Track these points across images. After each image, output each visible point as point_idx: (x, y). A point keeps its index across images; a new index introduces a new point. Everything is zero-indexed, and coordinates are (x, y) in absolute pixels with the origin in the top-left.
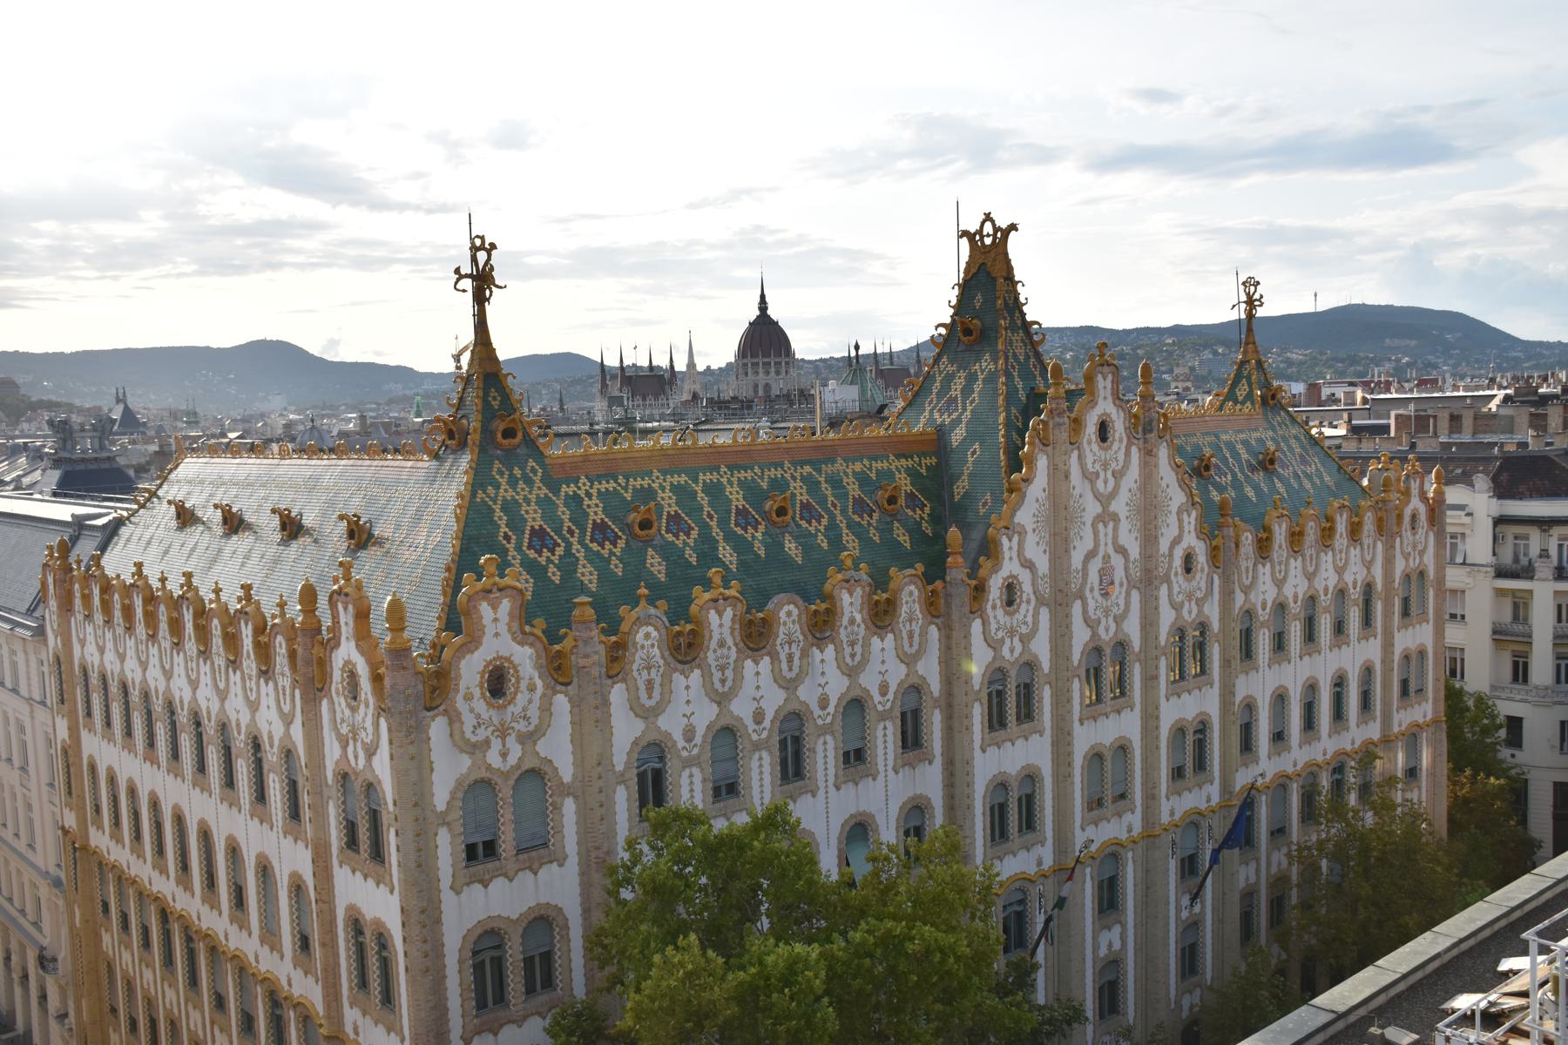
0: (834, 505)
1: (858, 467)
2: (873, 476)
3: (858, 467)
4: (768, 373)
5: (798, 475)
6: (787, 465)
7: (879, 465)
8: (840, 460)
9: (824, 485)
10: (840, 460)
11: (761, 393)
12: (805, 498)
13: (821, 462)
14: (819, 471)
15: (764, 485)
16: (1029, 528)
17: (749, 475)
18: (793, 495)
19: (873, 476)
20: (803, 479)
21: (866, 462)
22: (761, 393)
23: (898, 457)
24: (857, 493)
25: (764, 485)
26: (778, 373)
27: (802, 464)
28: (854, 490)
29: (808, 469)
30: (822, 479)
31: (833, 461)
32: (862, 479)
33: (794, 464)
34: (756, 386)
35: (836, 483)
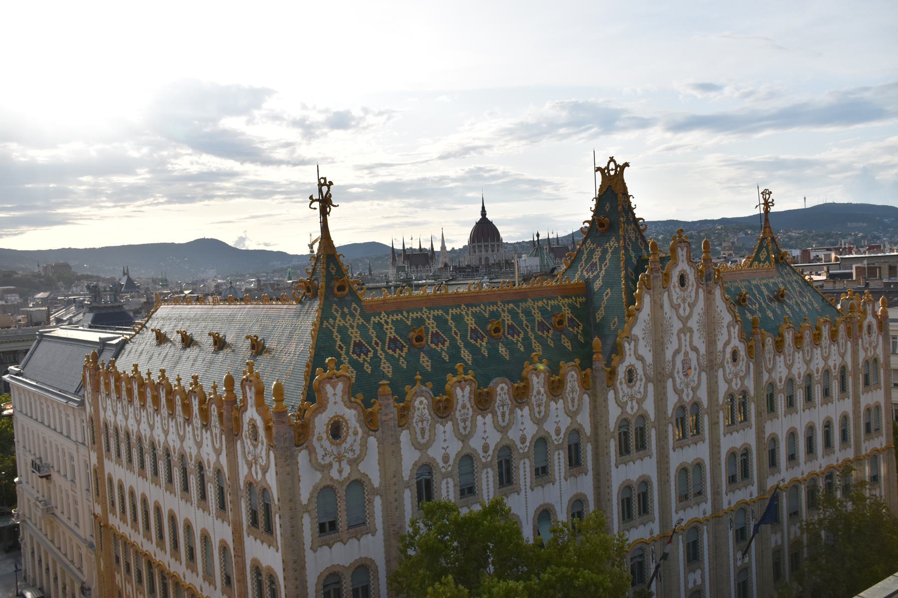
0: (527, 326)
1: (540, 304)
2: (549, 309)
3: (540, 304)
4: (487, 251)
5: (506, 309)
6: (499, 303)
7: (553, 302)
8: (530, 300)
9: (521, 315)
10: (530, 300)
11: (483, 263)
12: (510, 322)
14: (518, 307)
15: (487, 315)
16: (695, 330)
17: (478, 309)
18: (503, 320)
19: (549, 309)
20: (509, 311)
21: (545, 301)
22: (483, 263)
23: (563, 298)
24: (540, 319)
25: (487, 315)
26: (493, 251)
27: (508, 302)
28: (538, 317)
29: (511, 305)
31: (526, 301)
32: (543, 311)
33: (504, 303)
34: (481, 259)
35: (527, 313)
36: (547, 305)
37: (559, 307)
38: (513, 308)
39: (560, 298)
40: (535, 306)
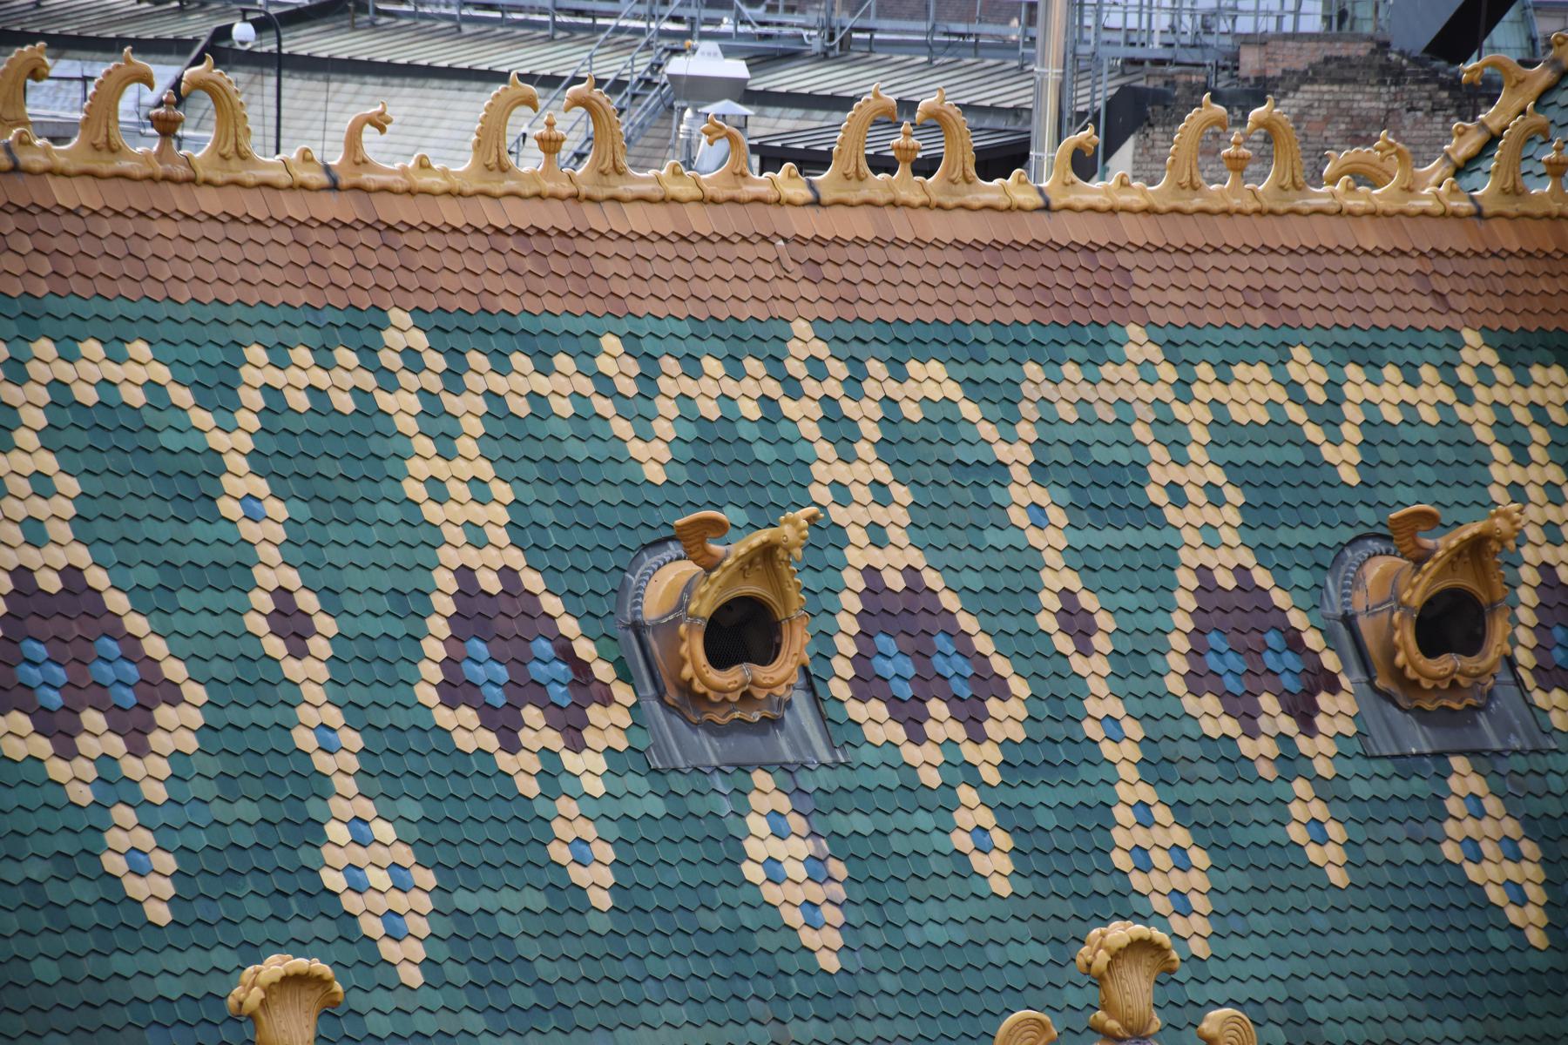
0: (1077, 623)
1: (1251, 394)
2: (1345, 459)
3: (1251, 394)
5: (865, 413)
6: (804, 342)
7: (1388, 393)
8: (1138, 344)
9: (1023, 492)
10: (1138, 344)
12: (898, 559)
13: (1019, 345)
14: (1003, 401)
15: (653, 460)
17: (563, 384)
18: (828, 536)
19: (1345, 459)
21: (1305, 367)
23: (1517, 350)
24: (1229, 558)
25: (653, 460)
27: (903, 344)
28: (1212, 539)
29: (932, 380)
30: (1015, 455)
31: (1098, 349)
32: (1275, 481)
33: (853, 340)
35: (1102, 485)
36: (1329, 415)
37: (1458, 458)
38: (944, 418)
39: (1476, 351)
40: (1193, 416)
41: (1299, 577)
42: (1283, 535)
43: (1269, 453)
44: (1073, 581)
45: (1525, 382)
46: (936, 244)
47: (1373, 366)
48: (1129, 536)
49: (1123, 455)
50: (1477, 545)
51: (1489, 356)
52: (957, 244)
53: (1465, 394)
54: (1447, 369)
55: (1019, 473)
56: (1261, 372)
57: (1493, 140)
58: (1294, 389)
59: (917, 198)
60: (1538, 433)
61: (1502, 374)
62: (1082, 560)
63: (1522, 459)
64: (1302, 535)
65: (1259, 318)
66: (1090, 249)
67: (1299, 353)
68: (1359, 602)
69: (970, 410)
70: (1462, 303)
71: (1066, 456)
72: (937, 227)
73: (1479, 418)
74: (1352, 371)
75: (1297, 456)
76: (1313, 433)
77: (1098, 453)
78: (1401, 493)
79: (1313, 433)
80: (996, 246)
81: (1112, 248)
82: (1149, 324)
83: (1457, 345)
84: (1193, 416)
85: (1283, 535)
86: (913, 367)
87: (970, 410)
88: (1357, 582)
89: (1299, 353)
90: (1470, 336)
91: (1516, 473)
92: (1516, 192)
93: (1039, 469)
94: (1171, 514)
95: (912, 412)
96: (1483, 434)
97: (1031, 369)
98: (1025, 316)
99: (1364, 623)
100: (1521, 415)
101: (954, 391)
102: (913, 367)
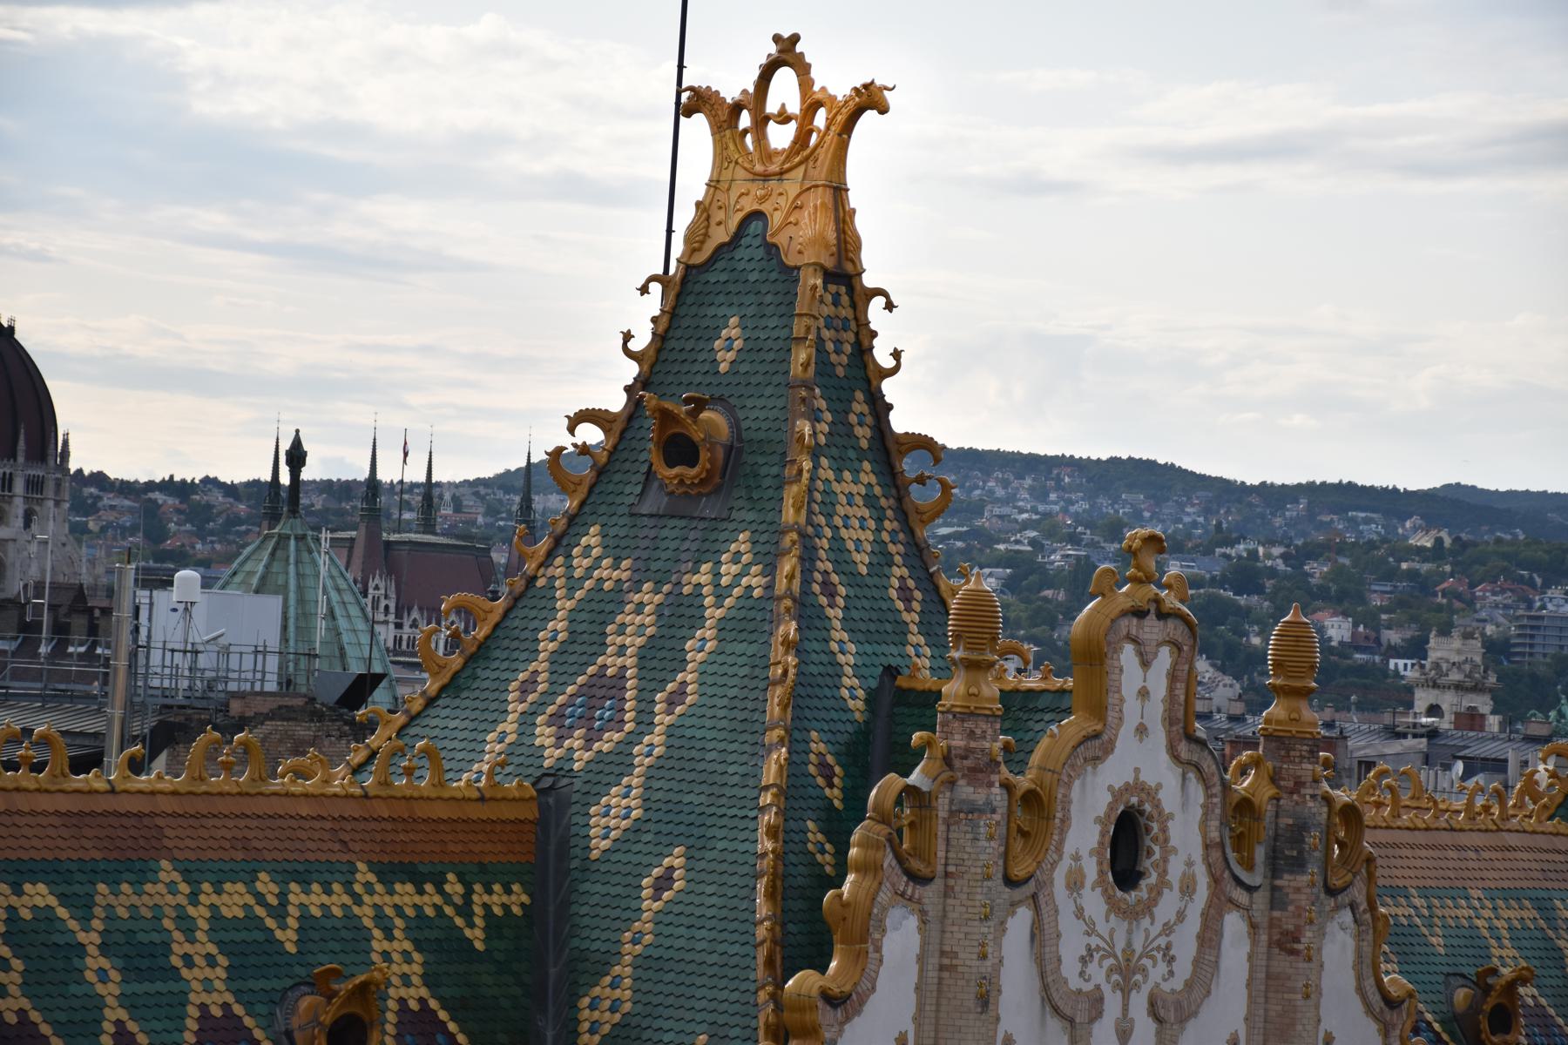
1: (234, 900)
2: (288, 938)
3: (234, 900)
8: (167, 871)
9: (95, 961)
10: (167, 871)
13: (95, 873)
14: (83, 907)
19: (288, 938)
21: (266, 884)
23: (388, 874)
28: (208, 986)
29: (39, 894)
30: (90, 939)
31: (142, 874)
32: (246, 950)
35: (142, 955)
36: (280, 913)
37: (352, 936)
38: (45, 916)
39: (364, 874)
40: (200, 914)
41: (261, 1009)
42: (251, 984)
43: (244, 935)
44: (122, 1014)
45: (391, 893)
46: (44, 813)
47: (305, 884)
48: (159, 986)
49: (156, 938)
50: (364, 988)
51: (372, 878)
52: (57, 813)
53: (358, 900)
54: (348, 886)
55: (92, 950)
56: (240, 887)
57: (373, 754)
58: (260, 898)
59: (33, 786)
60: (399, 922)
61: (379, 888)
62: (126, 1001)
63: (389, 937)
64: (262, 984)
65: (240, 855)
66: (139, 815)
67: (263, 876)
68: (295, 1022)
69: (62, 912)
70: (357, 847)
71: (121, 939)
72: (44, 803)
73: (365, 913)
74: (293, 886)
75: (259, 936)
76: (270, 923)
77: (141, 937)
78: (321, 958)
79: (270, 923)
80: (81, 814)
81: (152, 815)
82: (173, 860)
83: (354, 871)
84: (200, 914)
85: (251, 984)
86: (27, 887)
87: (62, 912)
88: (294, 1010)
89: (263, 876)
90: (361, 866)
91: (386, 945)
92: (386, 784)
93: (104, 948)
94: (185, 973)
95: (26, 914)
96: (367, 922)
97: (101, 887)
98: (98, 855)
99: (297, 1035)
100: (389, 911)
101: (52, 901)
102: (27, 887)
